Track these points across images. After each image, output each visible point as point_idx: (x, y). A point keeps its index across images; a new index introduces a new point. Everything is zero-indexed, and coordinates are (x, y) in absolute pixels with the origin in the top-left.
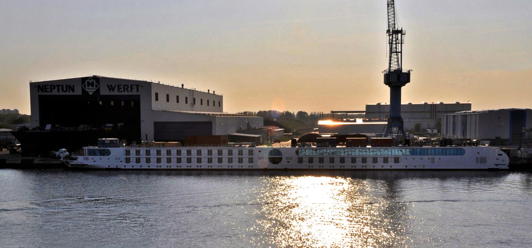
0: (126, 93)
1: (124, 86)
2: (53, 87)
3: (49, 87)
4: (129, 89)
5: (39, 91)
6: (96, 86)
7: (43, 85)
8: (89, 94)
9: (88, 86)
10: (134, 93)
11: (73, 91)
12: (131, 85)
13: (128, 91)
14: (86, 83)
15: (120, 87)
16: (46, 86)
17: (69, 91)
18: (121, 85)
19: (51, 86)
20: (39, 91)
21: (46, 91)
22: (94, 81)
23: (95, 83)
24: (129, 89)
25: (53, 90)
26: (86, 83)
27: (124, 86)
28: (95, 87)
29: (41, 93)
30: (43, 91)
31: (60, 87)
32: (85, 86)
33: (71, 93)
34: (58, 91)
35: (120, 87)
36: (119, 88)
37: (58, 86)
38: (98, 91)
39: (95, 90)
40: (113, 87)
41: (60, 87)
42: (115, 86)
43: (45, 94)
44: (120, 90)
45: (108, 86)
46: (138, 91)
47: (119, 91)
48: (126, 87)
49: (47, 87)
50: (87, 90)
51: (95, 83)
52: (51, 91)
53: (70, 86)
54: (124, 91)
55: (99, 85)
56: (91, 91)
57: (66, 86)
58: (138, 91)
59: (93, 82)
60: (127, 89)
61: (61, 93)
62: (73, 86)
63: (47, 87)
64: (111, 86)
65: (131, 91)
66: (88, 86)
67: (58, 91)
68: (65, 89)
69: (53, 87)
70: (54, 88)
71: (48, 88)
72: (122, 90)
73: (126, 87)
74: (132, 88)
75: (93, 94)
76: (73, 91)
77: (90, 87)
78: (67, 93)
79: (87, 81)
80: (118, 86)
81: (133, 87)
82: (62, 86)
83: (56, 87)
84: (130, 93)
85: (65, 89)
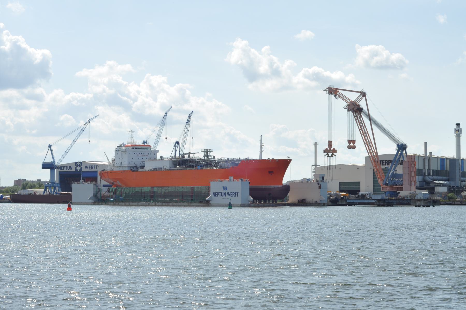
0: (92, 170)
4: (93, 168)
6: (81, 166)
8: (77, 170)
9: (78, 167)
10: (95, 170)
11: (72, 169)
12: (94, 166)
13: (93, 169)
14: (77, 165)
15: (90, 167)
18: (90, 166)
21: (62, 170)
22: (80, 164)
23: (80, 165)
24: (93, 168)
25: (64, 169)
26: (77, 165)
28: (80, 167)
30: (60, 169)
31: (67, 167)
32: (76, 167)
34: (66, 169)
35: (90, 167)
36: (89, 167)
37: (66, 167)
38: (81, 169)
39: (80, 169)
41: (67, 167)
44: (90, 168)
45: (85, 166)
46: (97, 169)
47: (89, 169)
48: (92, 167)
50: (77, 169)
51: (80, 165)
52: (64, 169)
53: (71, 166)
55: (82, 165)
56: (78, 169)
57: (69, 166)
58: (97, 169)
59: (79, 164)
60: (92, 168)
61: (67, 170)
62: (72, 166)
64: (86, 166)
65: (94, 169)
66: (78, 167)
67: (66, 169)
68: (69, 168)
72: (90, 168)
73: (92, 167)
74: (94, 167)
75: (79, 170)
76: (72, 169)
77: (78, 167)
79: (77, 164)
80: (89, 166)
81: (95, 167)
83: (66, 167)
85: (69, 169)
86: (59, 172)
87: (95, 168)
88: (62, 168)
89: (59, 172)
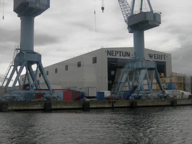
1: (158, 55)
2: (117, 53)
3: (114, 52)
5: (108, 55)
7: (110, 51)
10: (163, 60)
11: (129, 56)
16: (112, 51)
17: (127, 56)
19: (116, 51)
20: (108, 55)
21: (112, 55)
24: (160, 58)
27: (158, 55)
29: (109, 56)
30: (110, 55)
31: (121, 53)
33: (128, 58)
34: (120, 56)
37: (120, 52)
40: (152, 55)
41: (121, 53)
42: (153, 54)
43: (111, 57)
44: (156, 58)
46: (165, 59)
47: (155, 58)
48: (159, 56)
49: (113, 52)
52: (116, 56)
53: (127, 52)
54: (158, 59)
58: (165, 59)
60: (159, 57)
61: (122, 57)
62: (129, 52)
63: (113, 52)
64: (151, 54)
65: (161, 59)
67: (120, 56)
68: (124, 55)
69: (117, 53)
70: (118, 53)
71: (114, 53)
73: (159, 56)
74: (162, 57)
76: (129, 56)
78: (126, 58)
80: (155, 55)
81: (162, 56)
82: (123, 52)
83: (119, 53)
84: (160, 60)
85: (124, 55)
86: (108, 58)
87: (163, 58)
88: (112, 53)
89: (108, 58)
